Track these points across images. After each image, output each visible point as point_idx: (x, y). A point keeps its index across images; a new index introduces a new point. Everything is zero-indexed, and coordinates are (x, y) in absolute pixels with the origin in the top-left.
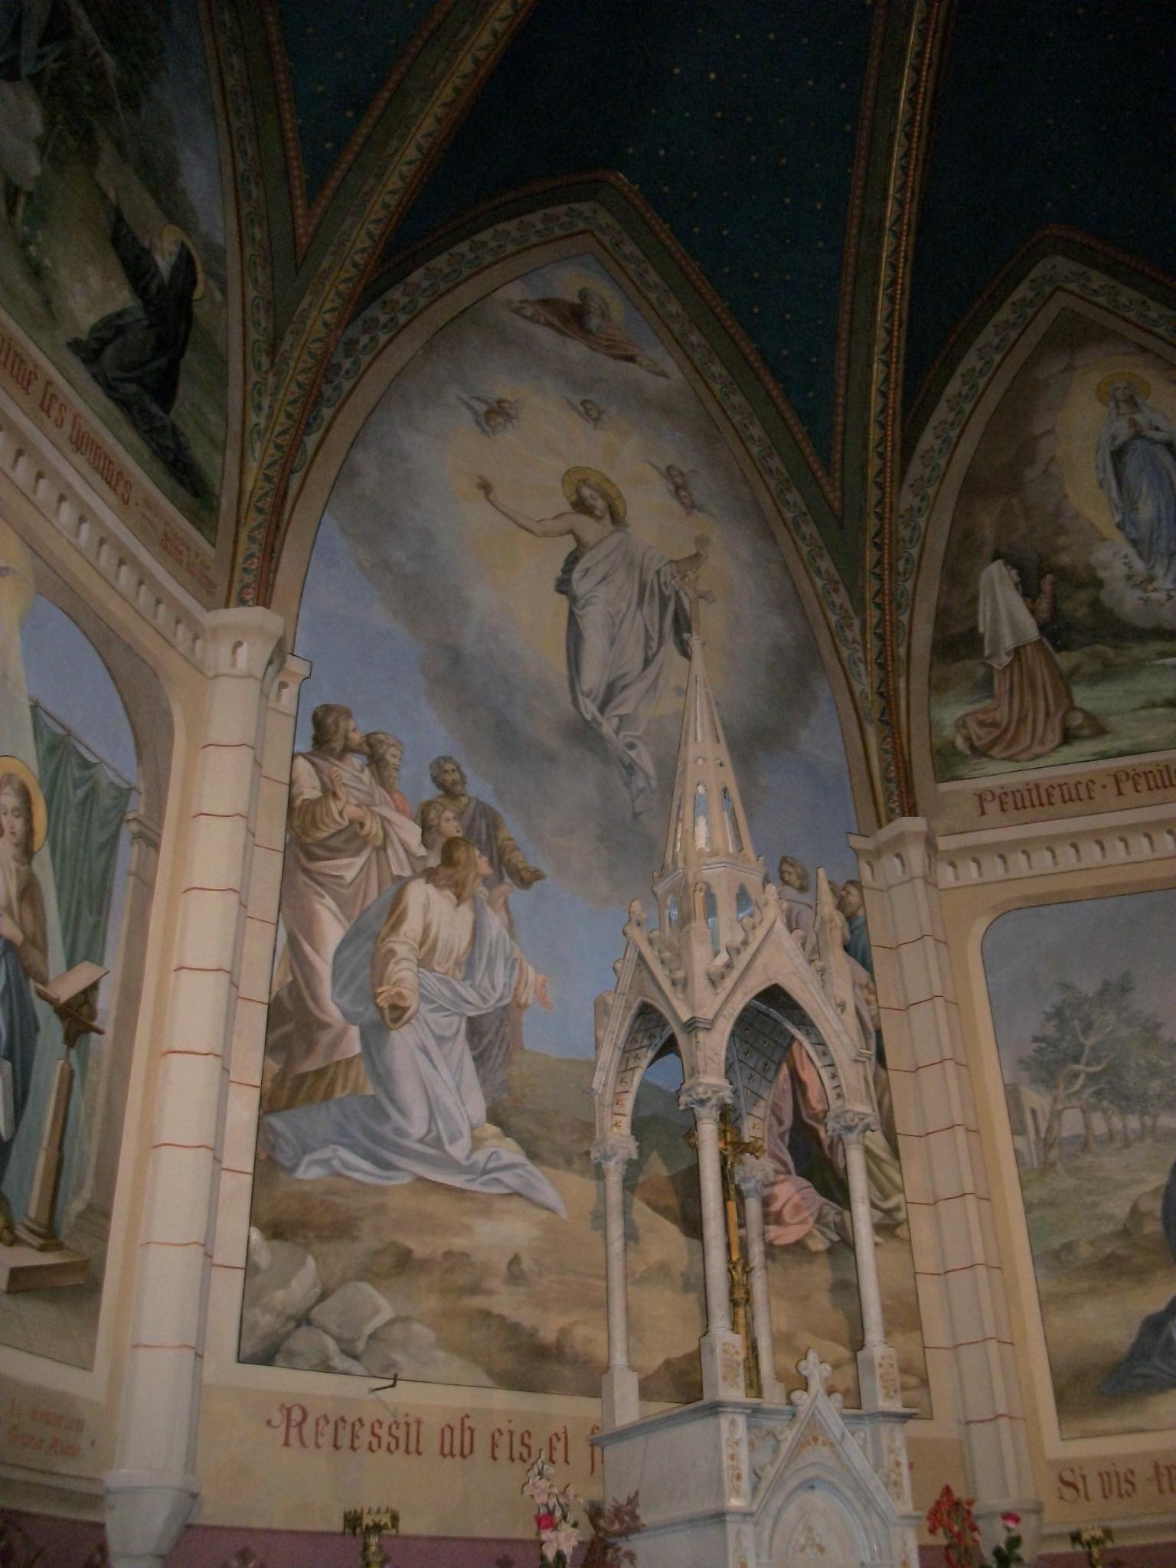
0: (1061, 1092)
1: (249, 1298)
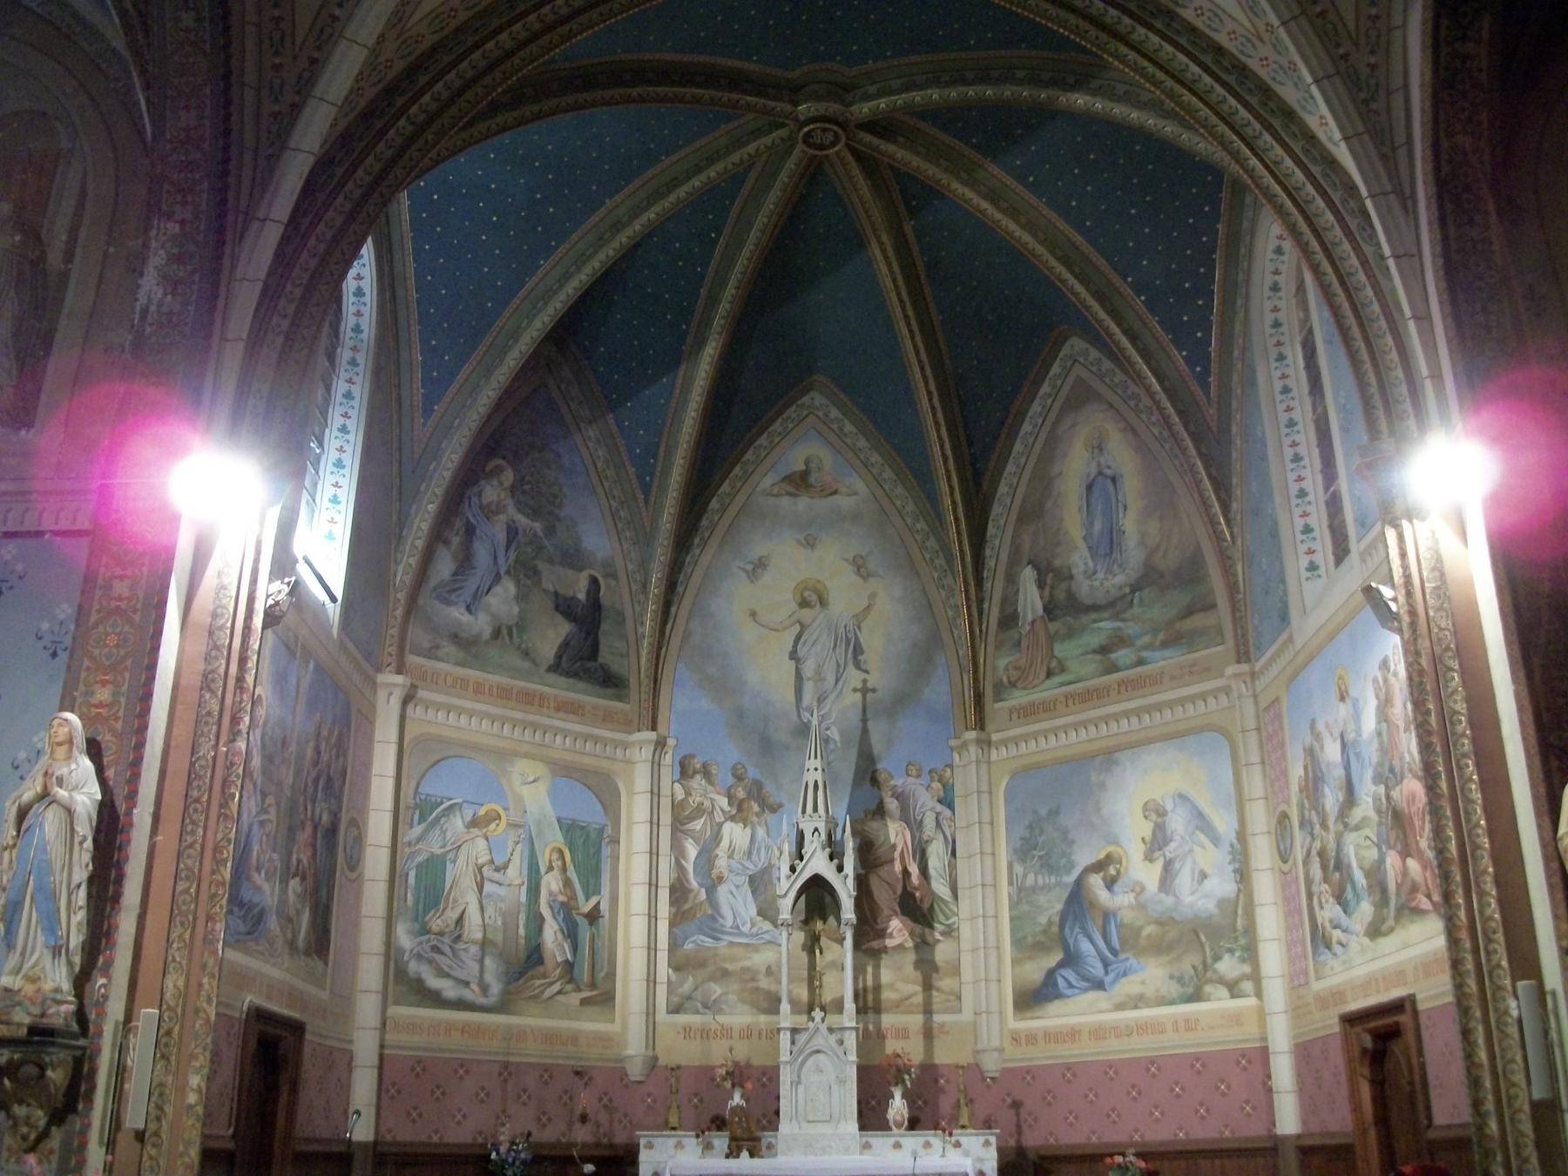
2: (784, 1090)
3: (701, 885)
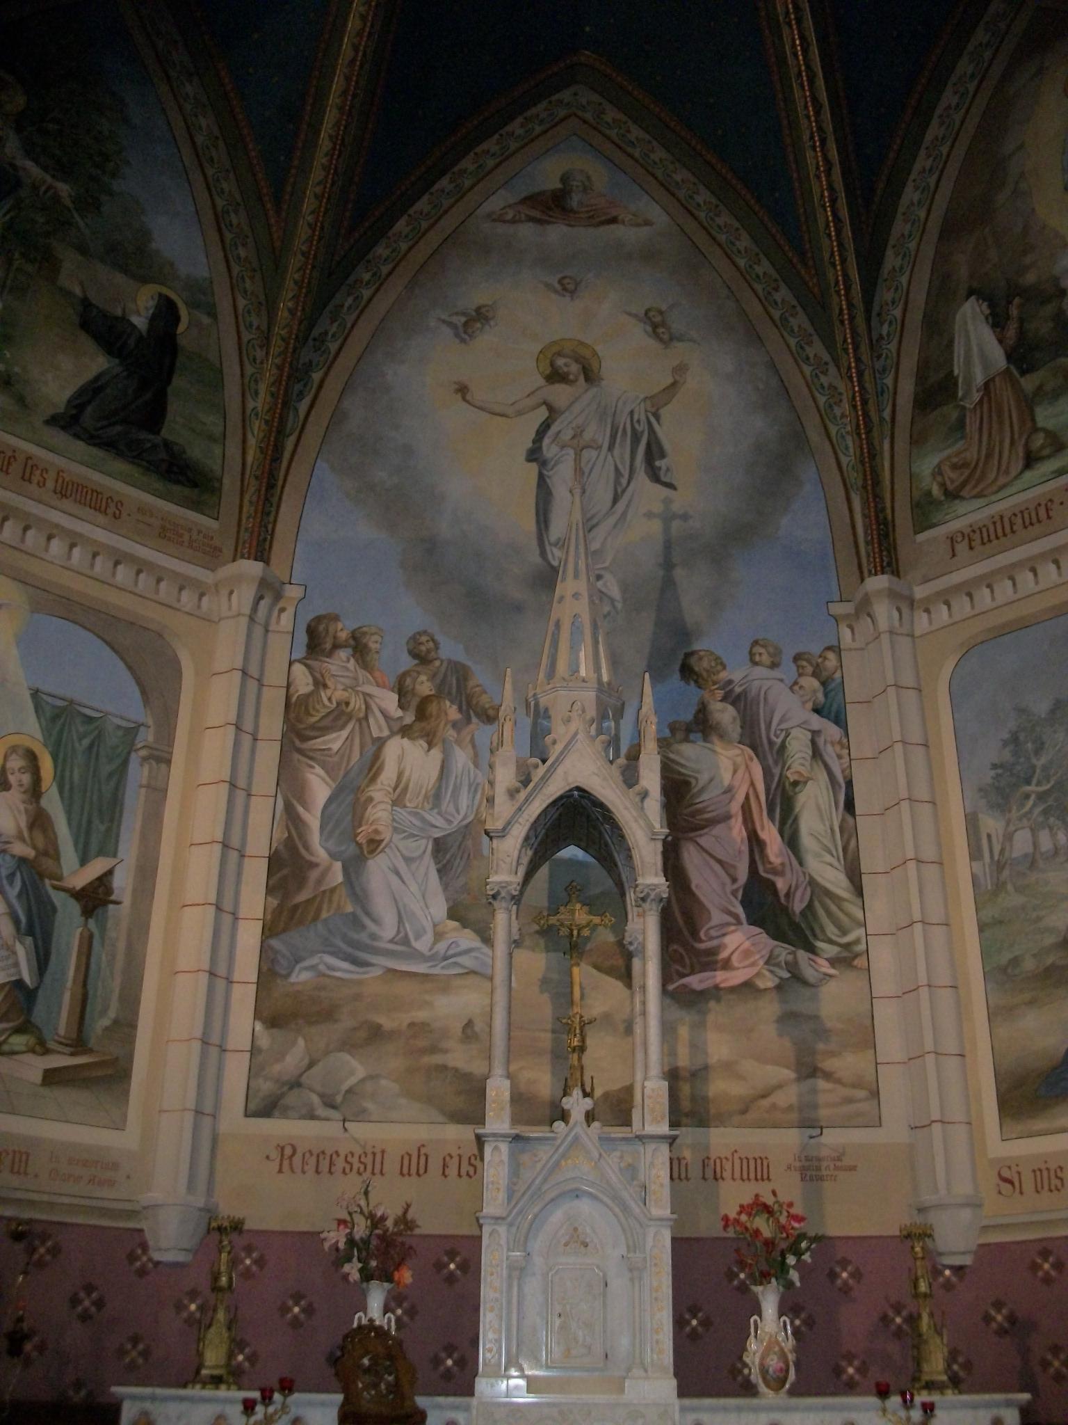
0: (1014, 814)
1: (254, 1072)
2: (491, 1289)
3: (333, 856)
